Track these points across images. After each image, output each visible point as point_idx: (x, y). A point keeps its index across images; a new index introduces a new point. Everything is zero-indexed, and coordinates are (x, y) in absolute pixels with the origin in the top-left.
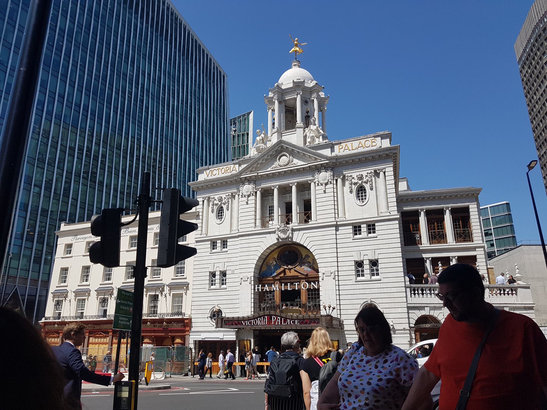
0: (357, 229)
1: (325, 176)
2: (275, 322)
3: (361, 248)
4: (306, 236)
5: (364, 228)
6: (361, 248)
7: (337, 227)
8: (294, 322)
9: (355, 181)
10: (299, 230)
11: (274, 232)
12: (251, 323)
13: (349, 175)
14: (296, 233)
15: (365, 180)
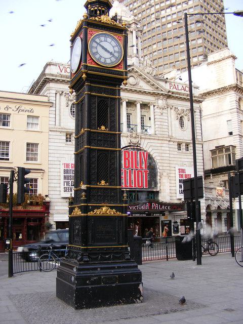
0: (179, 145)
1: (161, 102)
2: (154, 207)
3: (183, 160)
4: (149, 144)
5: (183, 147)
6: (183, 160)
7: (169, 141)
8: (167, 208)
9: (179, 112)
10: (145, 138)
11: (127, 137)
12: (136, 208)
13: (176, 107)
14: (143, 140)
15: (185, 113)
